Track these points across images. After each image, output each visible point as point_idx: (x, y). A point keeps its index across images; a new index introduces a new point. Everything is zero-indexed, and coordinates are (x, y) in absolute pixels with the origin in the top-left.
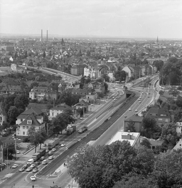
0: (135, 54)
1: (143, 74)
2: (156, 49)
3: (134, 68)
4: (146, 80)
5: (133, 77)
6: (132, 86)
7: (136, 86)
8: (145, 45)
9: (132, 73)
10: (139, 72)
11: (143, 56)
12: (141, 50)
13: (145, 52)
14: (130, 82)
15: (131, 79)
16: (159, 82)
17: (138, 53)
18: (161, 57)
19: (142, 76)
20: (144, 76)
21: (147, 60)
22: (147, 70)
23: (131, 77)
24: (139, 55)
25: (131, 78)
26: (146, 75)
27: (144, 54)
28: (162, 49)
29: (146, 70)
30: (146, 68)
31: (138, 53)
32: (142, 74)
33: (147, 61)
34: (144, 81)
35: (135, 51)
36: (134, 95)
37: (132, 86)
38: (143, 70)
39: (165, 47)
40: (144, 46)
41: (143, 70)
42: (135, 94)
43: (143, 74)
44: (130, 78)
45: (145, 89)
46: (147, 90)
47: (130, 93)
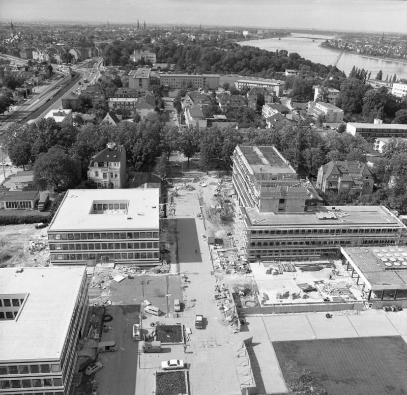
1: (90, 56)
2: (106, 32)
16: (102, 64)
18: (109, 40)
19: (88, 58)
27: (92, 37)
28: (112, 32)
29: (92, 52)
30: (92, 50)
34: (90, 62)
38: (90, 52)
39: (114, 31)
41: (90, 52)
43: (90, 56)
45: (90, 69)
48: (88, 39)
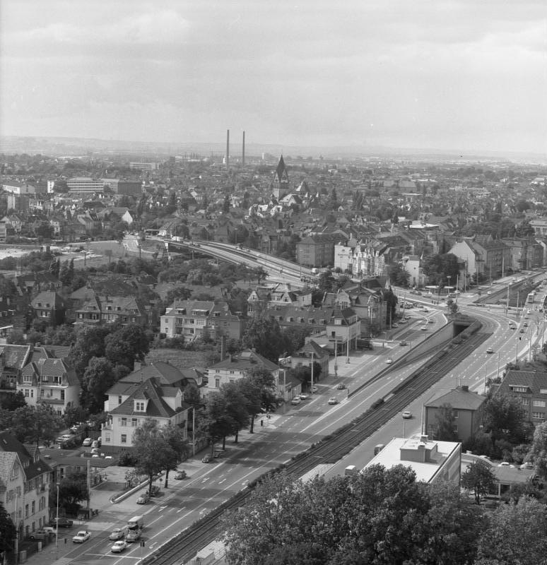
0: (499, 206)
1: (516, 265)
3: (486, 246)
4: (520, 284)
5: (483, 274)
6: (474, 302)
7: (489, 301)
8: (538, 177)
9: (478, 261)
10: (501, 260)
11: (524, 212)
12: (523, 194)
13: (533, 200)
14: (472, 288)
15: (475, 281)
17: (513, 201)
19: (510, 272)
20: (518, 271)
21: (531, 223)
22: (528, 255)
23: (475, 274)
24: (512, 207)
25: (475, 277)
26: (525, 269)
31: (513, 201)
32: (511, 264)
33: (530, 225)
34: (515, 287)
35: (502, 195)
36: (476, 327)
37: (474, 302)
38: (517, 254)
40: (533, 179)
41: (517, 254)
42: (481, 326)
43: (516, 266)
44: (473, 276)
45: (514, 310)
46: (518, 314)
47: (465, 324)
48: (509, 212)
